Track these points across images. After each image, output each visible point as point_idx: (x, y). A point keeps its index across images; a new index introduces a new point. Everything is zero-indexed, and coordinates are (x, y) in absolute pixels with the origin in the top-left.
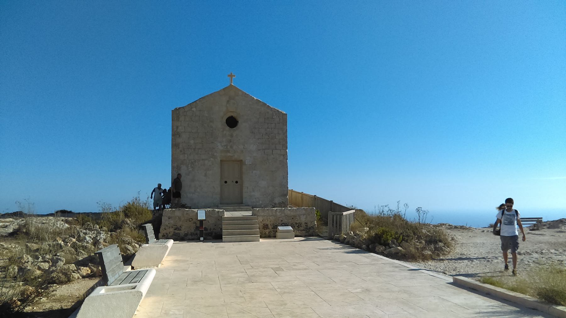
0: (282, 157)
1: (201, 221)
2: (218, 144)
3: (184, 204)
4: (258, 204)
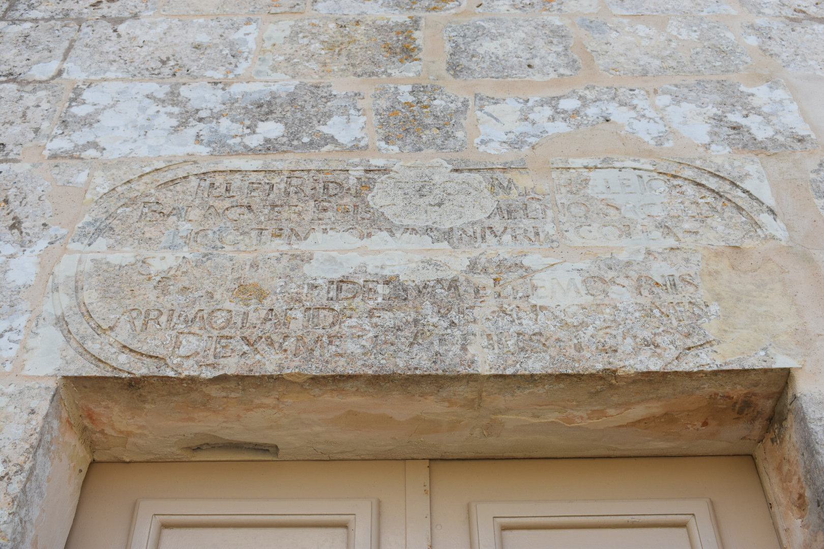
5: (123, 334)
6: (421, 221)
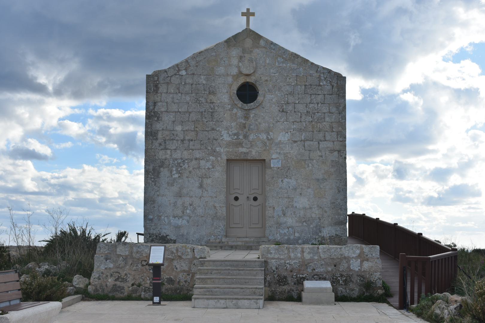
0: (336, 153)
1: (157, 268)
3: (165, 235)
4: (292, 237)
5: (229, 156)
6: (245, 147)
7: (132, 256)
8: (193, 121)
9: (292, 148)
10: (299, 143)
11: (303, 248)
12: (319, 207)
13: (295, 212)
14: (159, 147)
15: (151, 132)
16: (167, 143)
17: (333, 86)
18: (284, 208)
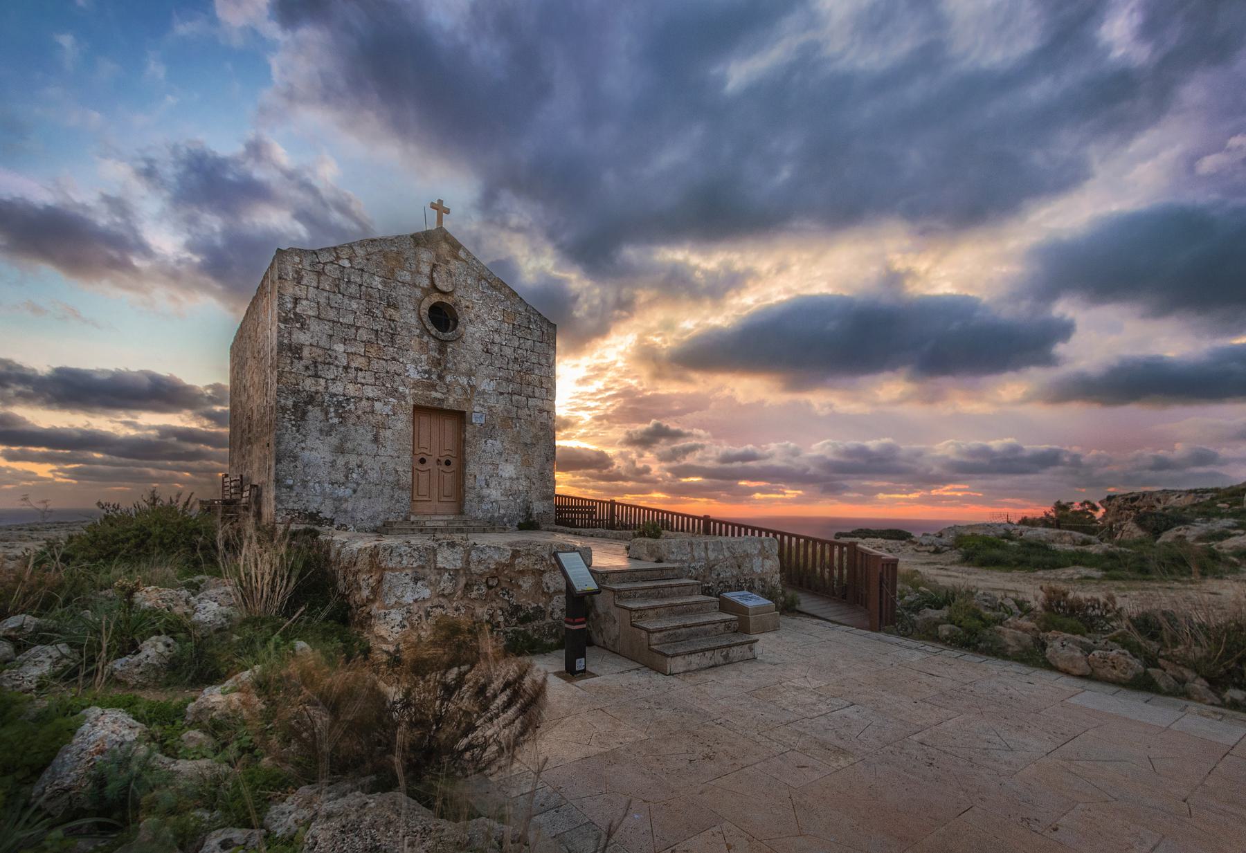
0: (545, 414)
2: (408, 366)
7: (469, 569)
8: (362, 342)
9: (498, 401)
10: (506, 395)
11: (706, 544)
12: (527, 478)
13: (500, 483)
14: (306, 371)
15: (290, 345)
16: (320, 367)
17: (543, 333)
18: (488, 477)
